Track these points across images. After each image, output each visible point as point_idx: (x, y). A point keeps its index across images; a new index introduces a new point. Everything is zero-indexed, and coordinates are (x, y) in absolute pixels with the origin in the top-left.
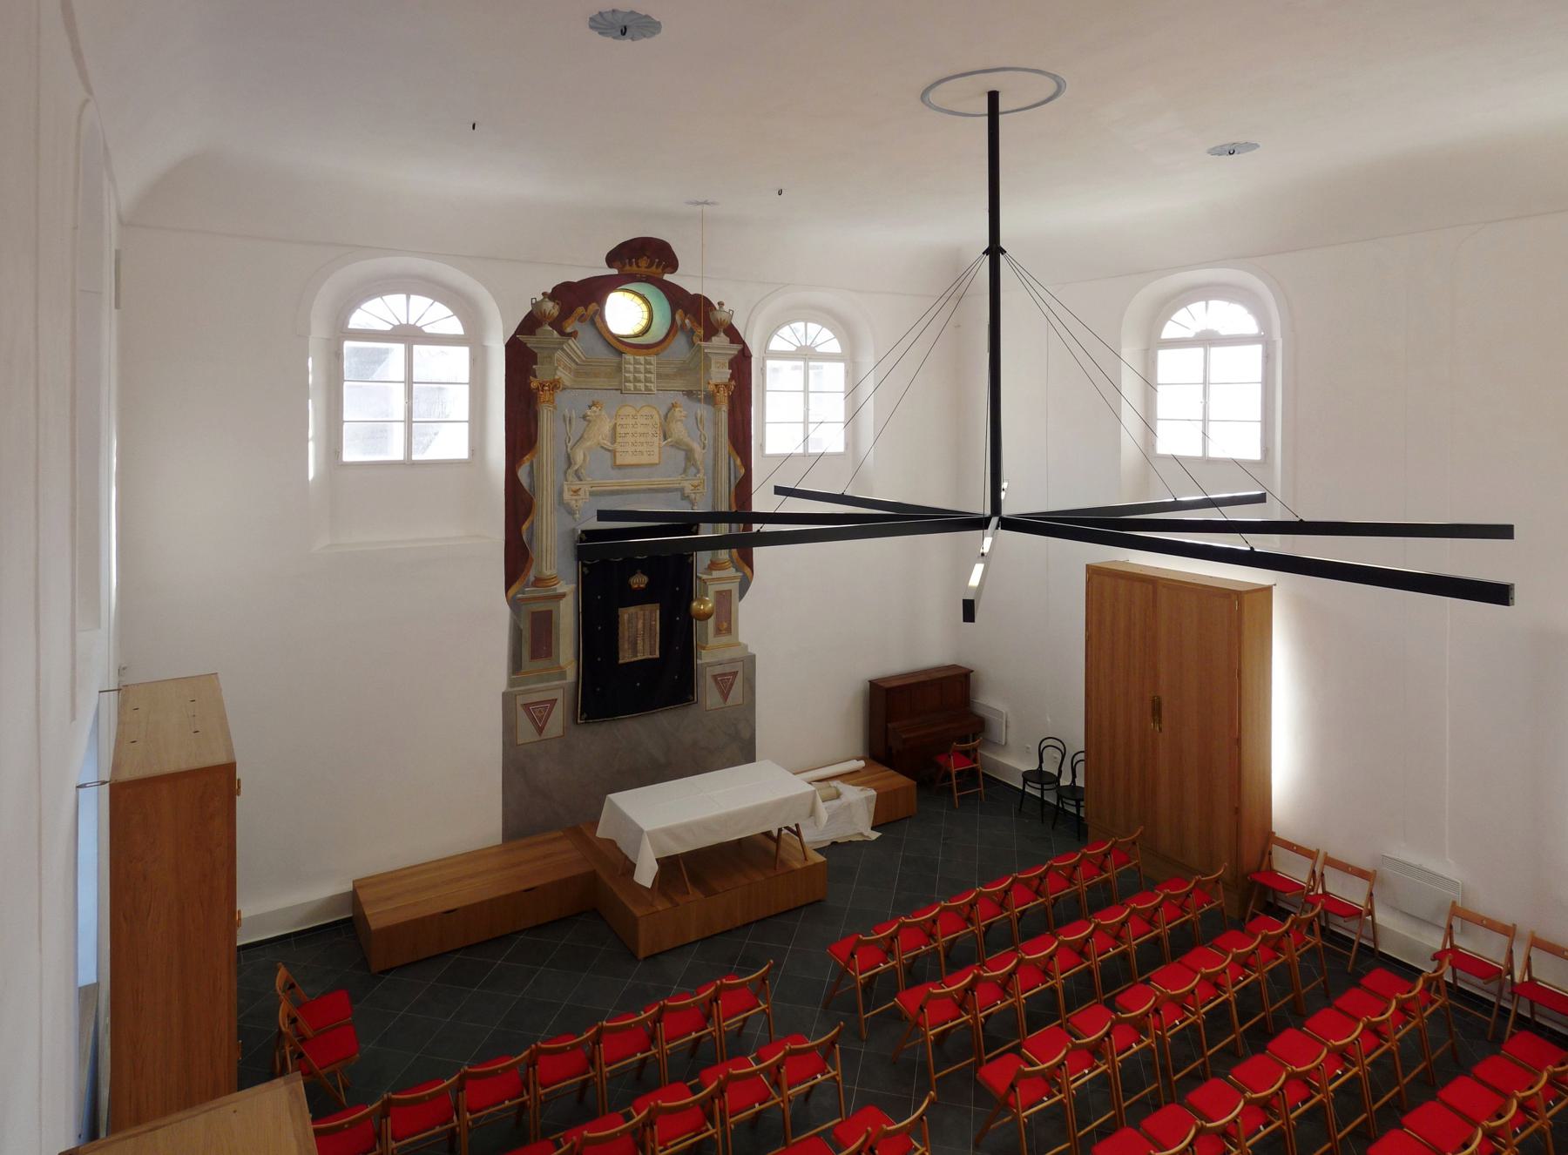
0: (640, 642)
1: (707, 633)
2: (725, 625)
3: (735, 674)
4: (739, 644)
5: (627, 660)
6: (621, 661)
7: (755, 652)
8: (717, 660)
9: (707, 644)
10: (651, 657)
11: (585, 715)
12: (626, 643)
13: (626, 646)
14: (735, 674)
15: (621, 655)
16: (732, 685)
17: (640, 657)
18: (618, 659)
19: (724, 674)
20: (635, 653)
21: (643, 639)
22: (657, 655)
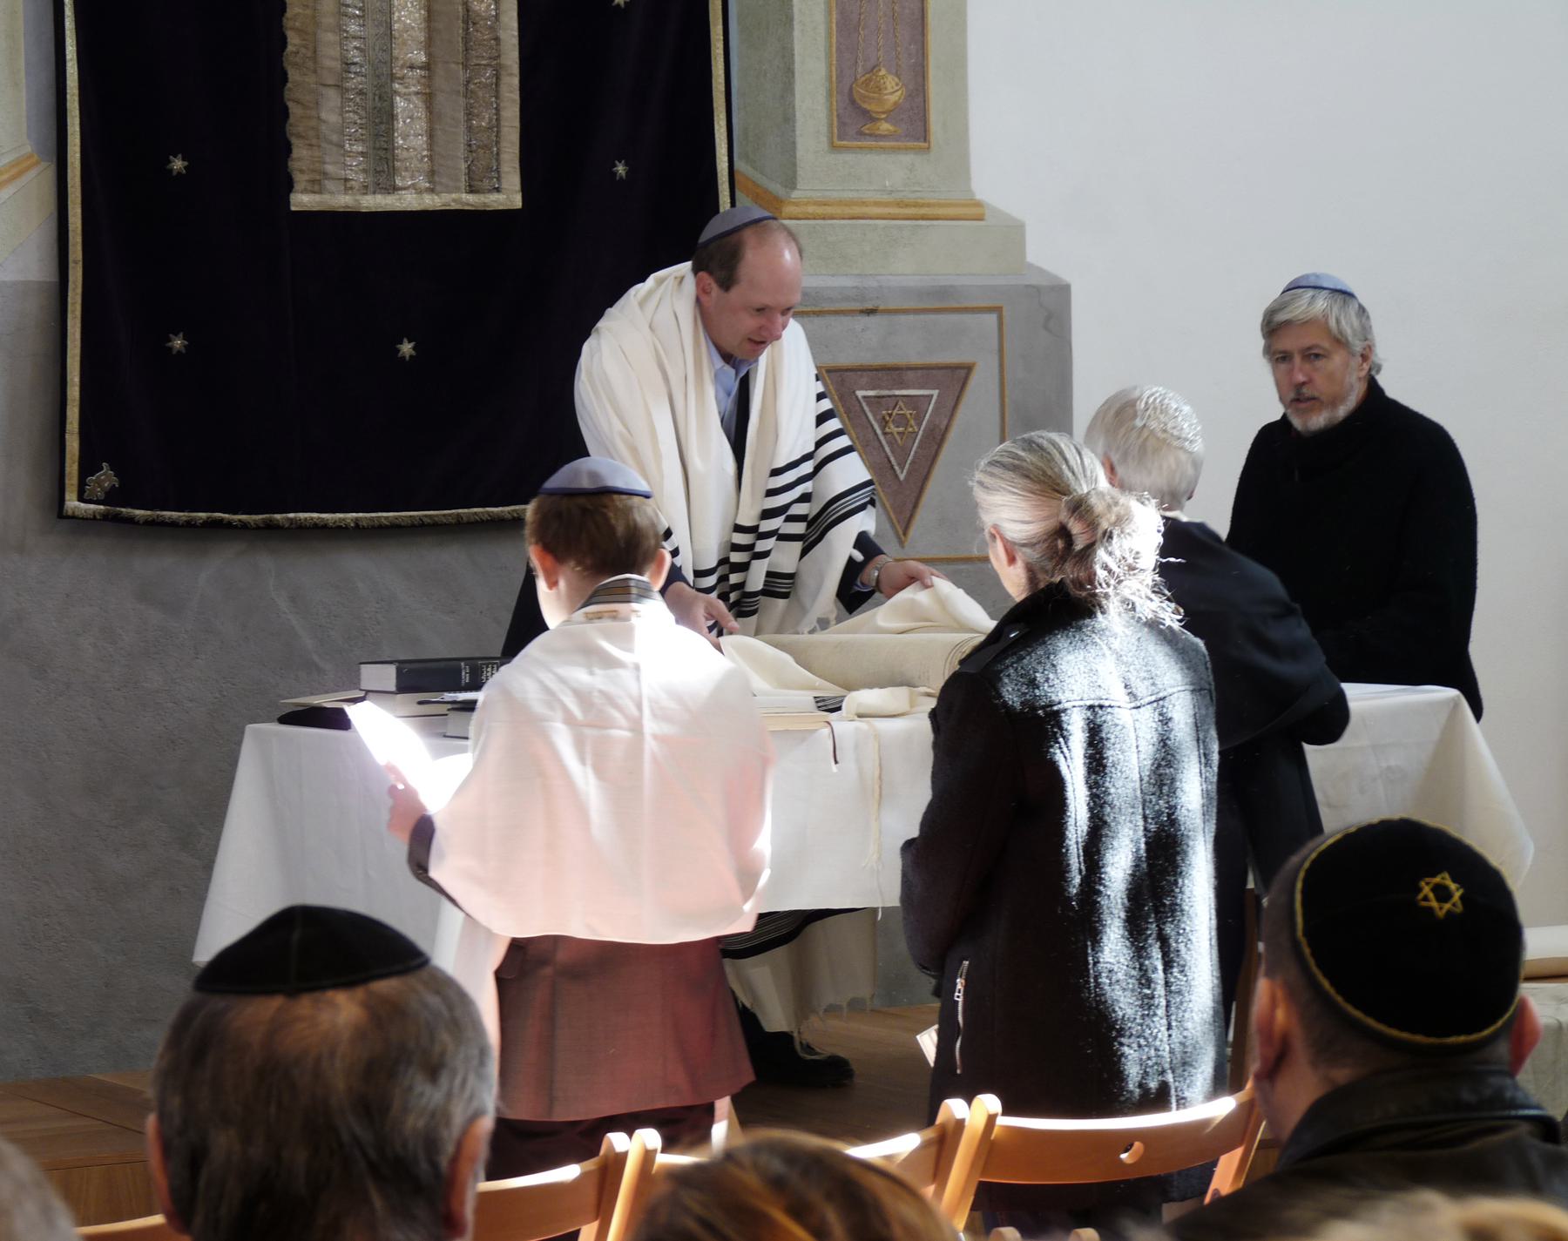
0: (408, 109)
1: (789, 119)
2: (893, 90)
3: (957, 377)
4: (975, 212)
5: (340, 200)
6: (302, 200)
7: (1065, 274)
8: (848, 282)
9: (791, 183)
10: (471, 201)
11: (106, 477)
12: (332, 98)
13: (330, 116)
14: (957, 377)
15: (301, 156)
16: (936, 438)
17: (408, 201)
18: (289, 185)
19: (894, 373)
20: (384, 169)
21: (429, 98)
22: (509, 196)
